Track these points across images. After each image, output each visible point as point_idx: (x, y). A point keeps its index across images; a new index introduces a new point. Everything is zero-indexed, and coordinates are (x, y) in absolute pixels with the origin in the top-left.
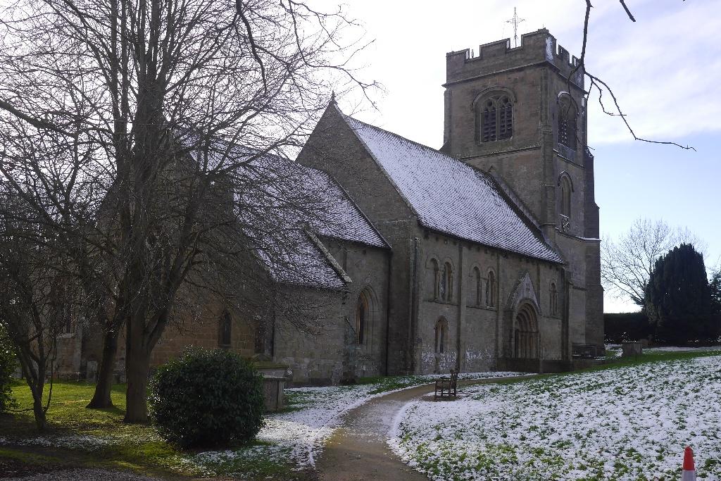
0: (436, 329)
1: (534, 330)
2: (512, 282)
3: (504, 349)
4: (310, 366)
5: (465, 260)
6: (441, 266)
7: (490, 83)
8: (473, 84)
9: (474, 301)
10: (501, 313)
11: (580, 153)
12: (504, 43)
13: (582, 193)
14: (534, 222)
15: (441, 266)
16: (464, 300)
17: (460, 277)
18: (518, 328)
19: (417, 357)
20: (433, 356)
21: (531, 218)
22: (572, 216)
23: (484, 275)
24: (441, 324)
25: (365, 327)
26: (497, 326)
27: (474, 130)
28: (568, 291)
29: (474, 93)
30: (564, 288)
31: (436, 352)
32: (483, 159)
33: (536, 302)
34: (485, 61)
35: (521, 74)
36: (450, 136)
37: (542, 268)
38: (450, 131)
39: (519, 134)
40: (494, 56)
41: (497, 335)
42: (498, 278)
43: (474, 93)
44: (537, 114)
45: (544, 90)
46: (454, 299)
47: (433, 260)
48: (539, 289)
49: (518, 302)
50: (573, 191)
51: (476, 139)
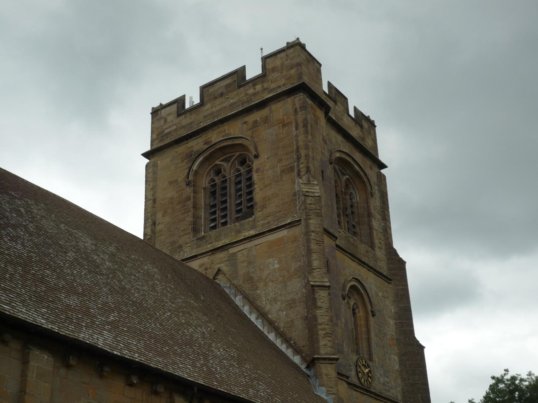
7: (215, 137)
11: (380, 254)
13: (392, 322)
14: (297, 359)
21: (289, 353)
27: (191, 214)
29: (192, 157)
34: (208, 106)
35: (265, 112)
36: (153, 232)
38: (154, 224)
39: (264, 207)
40: (222, 95)
43: (192, 157)
44: (292, 169)
45: (301, 129)
50: (373, 315)
51: (196, 230)
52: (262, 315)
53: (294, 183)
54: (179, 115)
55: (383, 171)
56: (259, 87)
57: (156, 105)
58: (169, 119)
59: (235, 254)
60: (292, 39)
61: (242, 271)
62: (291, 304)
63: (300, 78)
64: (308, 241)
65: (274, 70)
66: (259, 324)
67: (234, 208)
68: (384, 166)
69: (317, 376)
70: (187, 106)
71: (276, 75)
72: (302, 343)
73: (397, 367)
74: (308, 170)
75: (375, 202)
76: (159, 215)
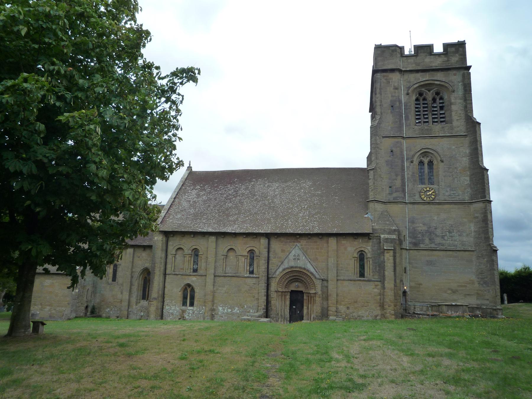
4: (50, 310)
20: (178, 309)
33: (312, 270)
37: (333, 241)
49: (281, 269)
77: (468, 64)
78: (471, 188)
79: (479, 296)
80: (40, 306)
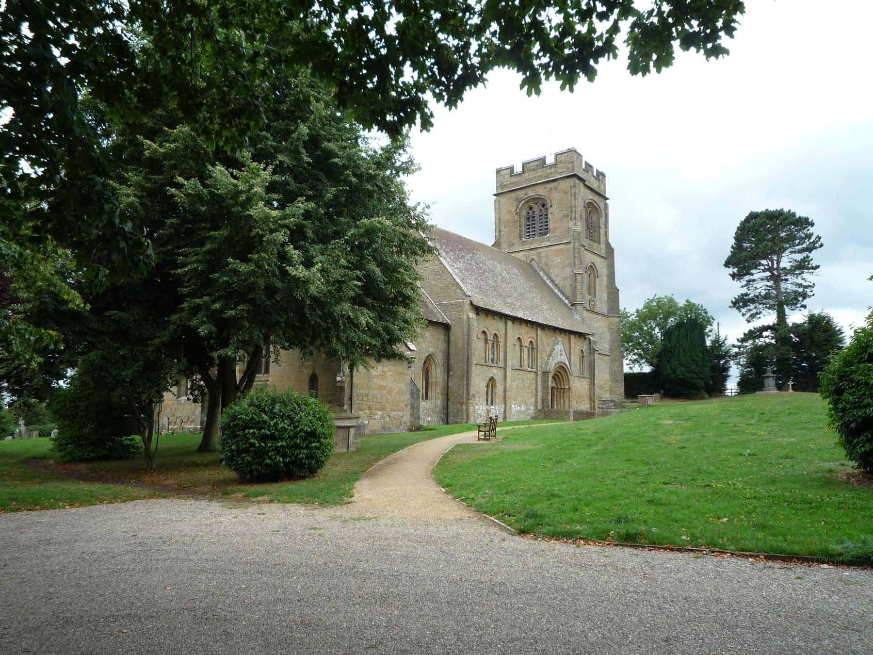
0: (487, 386)
1: (567, 387)
2: (548, 349)
3: (543, 402)
4: (382, 417)
5: (510, 331)
6: (490, 337)
7: (531, 193)
8: (517, 193)
9: (517, 365)
10: (540, 373)
11: (603, 246)
12: (543, 160)
13: (606, 278)
14: (567, 302)
15: (490, 337)
16: (509, 363)
17: (506, 346)
18: (554, 385)
19: (471, 409)
20: (485, 408)
21: (564, 298)
22: (597, 296)
23: (526, 343)
24: (491, 383)
25: (430, 387)
26: (537, 385)
28: (594, 356)
29: (518, 200)
30: (590, 353)
31: (487, 404)
32: (526, 253)
34: (527, 174)
35: (555, 184)
37: (572, 337)
39: (554, 232)
40: (534, 170)
41: (537, 391)
42: (537, 346)
44: (568, 216)
45: (573, 197)
46: (501, 364)
47: (484, 332)
48: (570, 354)
51: (520, 237)
52: (552, 281)
53: (568, 223)
54: (511, 176)
55: (607, 201)
56: (553, 170)
57: (499, 167)
58: (506, 177)
59: (540, 252)
60: (570, 147)
61: (543, 261)
62: (565, 278)
63: (573, 169)
64: (574, 253)
65: (561, 162)
66: (550, 285)
67: (539, 228)
68: (607, 199)
69: (576, 310)
70: (515, 171)
71: (562, 165)
72: (569, 295)
73: (606, 299)
74: (575, 219)
75: (602, 220)
76: (502, 227)
77: (607, 196)
78: (608, 304)
79: (611, 391)
80: (368, 412)
